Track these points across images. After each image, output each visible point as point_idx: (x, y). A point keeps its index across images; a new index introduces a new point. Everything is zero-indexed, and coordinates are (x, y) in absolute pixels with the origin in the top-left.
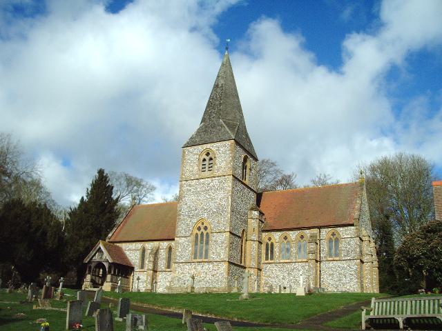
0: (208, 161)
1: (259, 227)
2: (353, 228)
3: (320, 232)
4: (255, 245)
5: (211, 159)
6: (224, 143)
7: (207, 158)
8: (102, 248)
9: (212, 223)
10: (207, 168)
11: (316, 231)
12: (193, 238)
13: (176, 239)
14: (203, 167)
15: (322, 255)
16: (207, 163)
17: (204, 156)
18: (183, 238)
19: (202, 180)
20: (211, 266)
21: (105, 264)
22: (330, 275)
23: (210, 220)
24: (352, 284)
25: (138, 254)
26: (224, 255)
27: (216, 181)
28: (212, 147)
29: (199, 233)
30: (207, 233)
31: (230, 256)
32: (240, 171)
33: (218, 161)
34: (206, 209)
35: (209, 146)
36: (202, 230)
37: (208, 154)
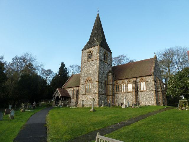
0: (90, 55)
1: (112, 79)
2: (151, 77)
3: (137, 79)
4: (111, 86)
5: (91, 54)
7: (90, 54)
8: (58, 91)
11: (135, 79)
15: (138, 89)
16: (90, 56)
17: (89, 53)
21: (59, 96)
22: (142, 98)
25: (72, 92)
26: (97, 91)
27: (93, 62)
28: (92, 49)
31: (99, 91)
32: (103, 58)
33: (94, 54)
35: (90, 49)
37: (90, 52)
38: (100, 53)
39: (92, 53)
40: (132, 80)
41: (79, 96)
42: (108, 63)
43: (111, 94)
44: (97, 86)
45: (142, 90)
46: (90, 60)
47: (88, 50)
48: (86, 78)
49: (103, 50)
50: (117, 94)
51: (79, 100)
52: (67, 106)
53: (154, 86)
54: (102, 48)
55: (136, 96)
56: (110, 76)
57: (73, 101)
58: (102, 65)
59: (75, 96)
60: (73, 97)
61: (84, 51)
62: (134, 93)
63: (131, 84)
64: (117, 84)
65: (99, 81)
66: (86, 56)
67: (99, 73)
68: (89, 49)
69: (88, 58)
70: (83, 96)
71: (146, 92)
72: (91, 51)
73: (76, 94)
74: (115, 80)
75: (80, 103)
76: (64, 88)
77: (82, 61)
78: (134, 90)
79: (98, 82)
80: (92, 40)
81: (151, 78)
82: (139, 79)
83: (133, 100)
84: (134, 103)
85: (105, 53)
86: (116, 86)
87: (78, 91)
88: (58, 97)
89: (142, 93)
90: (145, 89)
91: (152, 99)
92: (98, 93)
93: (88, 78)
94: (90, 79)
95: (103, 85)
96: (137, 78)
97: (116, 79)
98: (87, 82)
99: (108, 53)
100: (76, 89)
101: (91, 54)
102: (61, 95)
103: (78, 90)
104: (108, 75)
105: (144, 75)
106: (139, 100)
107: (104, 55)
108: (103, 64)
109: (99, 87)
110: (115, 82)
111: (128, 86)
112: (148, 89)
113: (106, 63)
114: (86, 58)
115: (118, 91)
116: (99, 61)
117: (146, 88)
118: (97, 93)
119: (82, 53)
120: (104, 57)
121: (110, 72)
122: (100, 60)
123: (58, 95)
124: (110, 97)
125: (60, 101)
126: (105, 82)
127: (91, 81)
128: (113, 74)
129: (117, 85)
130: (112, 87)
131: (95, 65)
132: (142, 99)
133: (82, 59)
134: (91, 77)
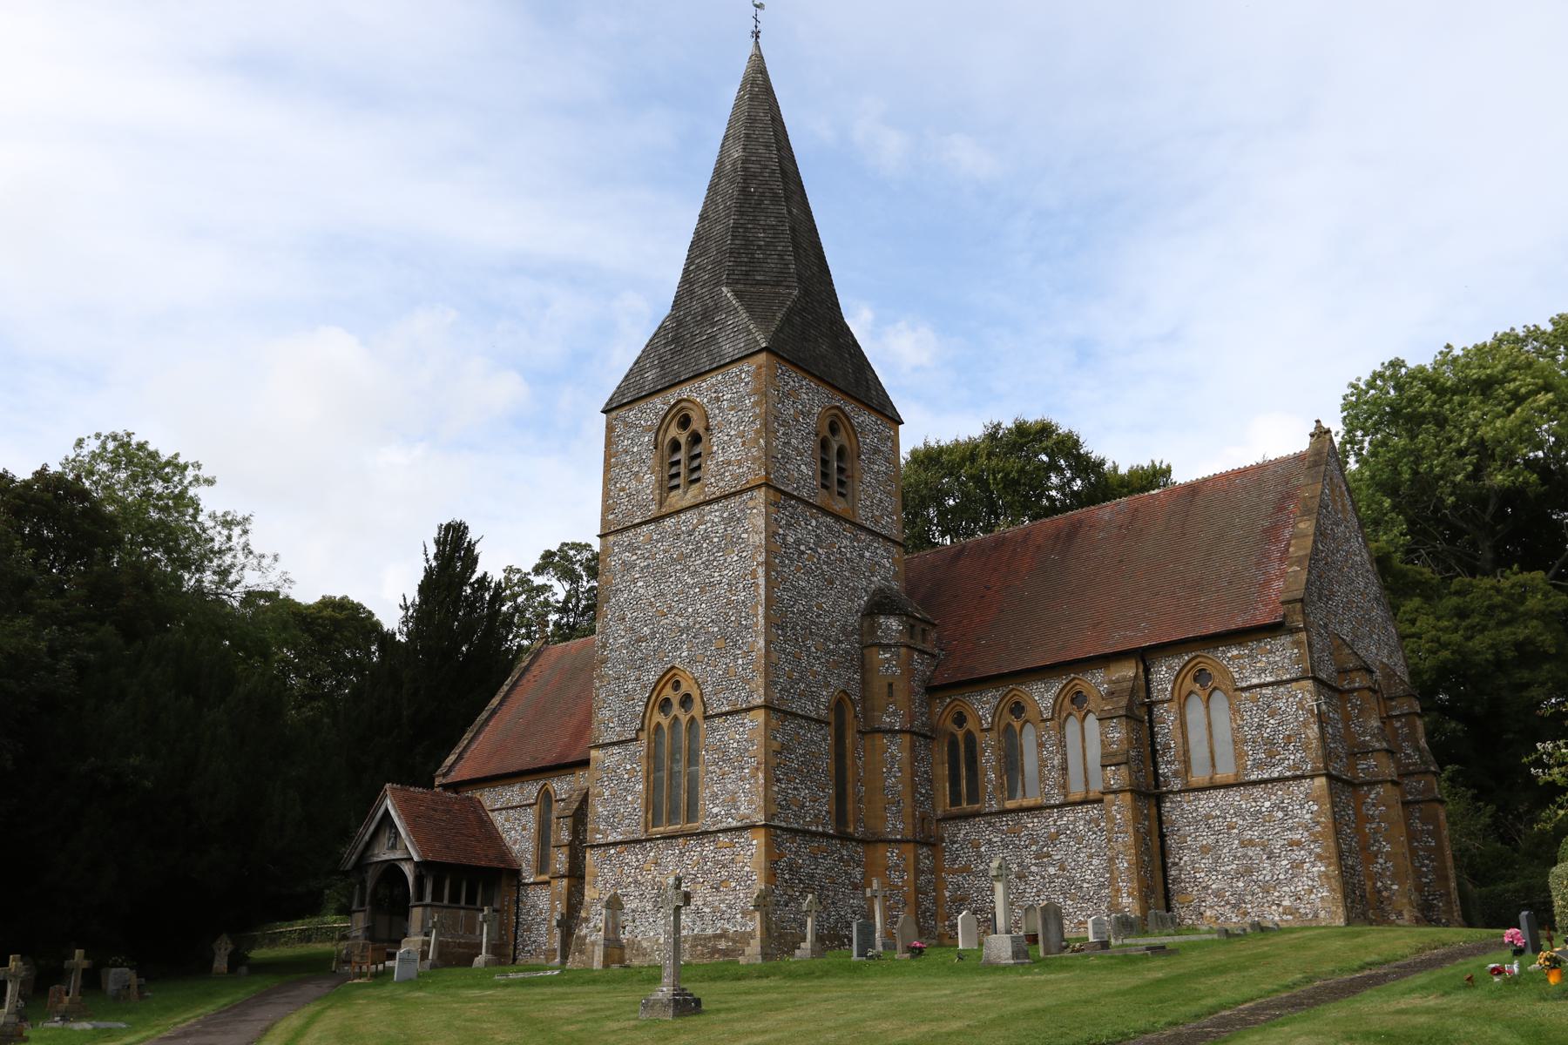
1: (909, 672)
3: (1147, 671)
4: (897, 750)
6: (734, 369)
7: (683, 438)
8: (392, 812)
9: (701, 675)
10: (682, 469)
11: (1128, 671)
12: (641, 748)
13: (594, 753)
14: (674, 470)
15: (1163, 769)
16: (681, 455)
17: (674, 432)
18: (616, 750)
19: (669, 522)
20: (709, 849)
22: (1205, 850)
23: (697, 670)
24: (1302, 885)
25: (530, 818)
26: (751, 807)
27: (714, 514)
28: (698, 393)
29: (665, 722)
30: (692, 719)
32: (804, 471)
33: (717, 438)
34: (688, 628)
35: (685, 391)
36: (676, 710)
37: (685, 422)
38: (771, 423)
39: (697, 425)
40: (1098, 682)
41: (591, 858)
42: (862, 516)
43: (894, 825)
44: (757, 748)
45: (1199, 775)
46: (676, 499)
47: (659, 404)
48: (653, 678)
49: (813, 399)
50: (964, 830)
51: (590, 893)
52: (480, 960)
53: (1313, 731)
54: (794, 379)
55: (1141, 839)
56: (887, 647)
57: (544, 903)
58: (798, 542)
59: (560, 861)
60: (543, 864)
61: (631, 414)
62: (1121, 809)
63: (1092, 722)
64: (960, 719)
65: (768, 707)
66: (650, 457)
67: (777, 621)
68: (672, 396)
69: (668, 485)
70: (631, 858)
71: (1236, 797)
72: (694, 415)
73: (565, 836)
74: (933, 690)
75: (593, 929)
76: (456, 787)
77: (607, 509)
78: (1117, 777)
79: (760, 716)
80: (696, 306)
81: (1281, 656)
82: (1164, 674)
83: (1112, 881)
84: (1129, 904)
85: (833, 429)
86: (953, 745)
87: (580, 816)
88: (392, 871)
89: (1205, 804)
90: (1226, 772)
91: (1297, 865)
92: (770, 816)
93: (670, 677)
94: (684, 688)
95: (822, 741)
96: (1145, 656)
97: (946, 677)
98: (658, 717)
99: (864, 418)
100: (561, 787)
101: (696, 439)
102: (421, 852)
103: (585, 800)
104: (869, 641)
105: (1212, 629)
106: (1173, 872)
107: (824, 445)
108: (809, 528)
109: (777, 765)
110: (942, 708)
111: (1062, 744)
112: (1259, 765)
113: (838, 518)
114: (649, 478)
115: (974, 796)
116: (768, 504)
117: (1239, 756)
118: (760, 819)
119: (610, 429)
120: (825, 463)
121: (881, 604)
122: (780, 495)
123: (398, 855)
124: (892, 855)
125: (416, 914)
126: (839, 706)
127: (697, 710)
128: (914, 627)
129: (960, 734)
130: (914, 757)
131: (732, 542)
132: (1206, 862)
133: (606, 495)
134: (692, 661)
